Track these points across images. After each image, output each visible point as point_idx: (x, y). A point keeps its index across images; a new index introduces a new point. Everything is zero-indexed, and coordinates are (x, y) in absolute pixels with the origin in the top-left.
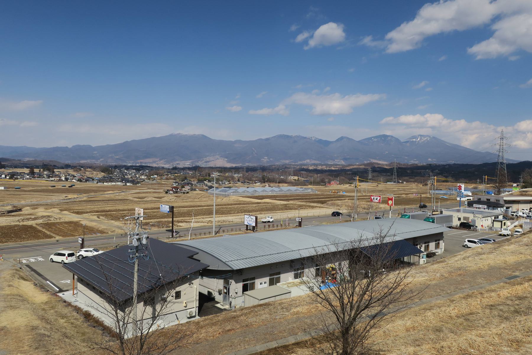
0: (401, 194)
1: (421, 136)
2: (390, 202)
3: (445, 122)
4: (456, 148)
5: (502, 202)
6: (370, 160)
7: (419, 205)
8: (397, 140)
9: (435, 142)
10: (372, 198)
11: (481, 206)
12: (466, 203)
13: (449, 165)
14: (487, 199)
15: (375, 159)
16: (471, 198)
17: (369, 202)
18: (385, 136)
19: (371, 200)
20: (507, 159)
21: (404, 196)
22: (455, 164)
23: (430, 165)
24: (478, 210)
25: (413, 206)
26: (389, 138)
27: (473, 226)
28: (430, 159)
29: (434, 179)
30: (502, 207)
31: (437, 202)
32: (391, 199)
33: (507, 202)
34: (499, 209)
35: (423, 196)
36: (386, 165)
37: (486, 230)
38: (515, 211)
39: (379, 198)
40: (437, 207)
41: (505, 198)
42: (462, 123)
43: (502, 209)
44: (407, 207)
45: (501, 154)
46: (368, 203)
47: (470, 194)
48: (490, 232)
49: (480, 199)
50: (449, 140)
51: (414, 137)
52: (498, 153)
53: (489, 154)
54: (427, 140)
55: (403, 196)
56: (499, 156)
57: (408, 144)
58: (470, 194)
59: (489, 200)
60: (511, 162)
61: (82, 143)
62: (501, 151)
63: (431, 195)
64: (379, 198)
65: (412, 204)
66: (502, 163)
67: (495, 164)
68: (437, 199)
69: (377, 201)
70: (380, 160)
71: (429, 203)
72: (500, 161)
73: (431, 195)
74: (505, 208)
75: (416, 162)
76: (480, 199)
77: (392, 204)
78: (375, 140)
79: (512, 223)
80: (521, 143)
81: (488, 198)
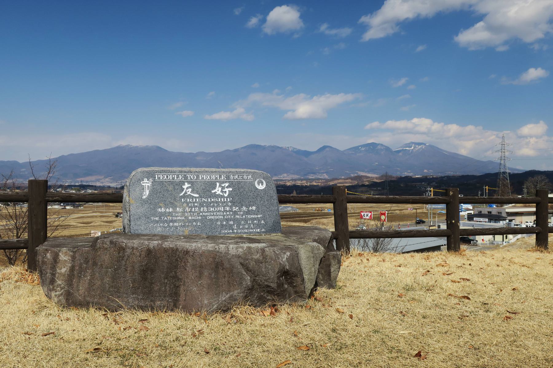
0: (395, 210)
1: (416, 144)
2: (383, 217)
3: (436, 127)
4: (455, 157)
5: (504, 215)
6: (357, 173)
7: (414, 221)
8: (387, 149)
9: (433, 150)
10: (362, 214)
11: (481, 219)
12: (466, 217)
13: (448, 177)
14: (488, 212)
15: (363, 171)
16: (472, 212)
17: (358, 219)
18: (374, 145)
19: (361, 217)
20: (509, 169)
21: (398, 212)
22: (453, 176)
23: (426, 177)
24: (478, 223)
25: (408, 223)
26: (379, 147)
27: (473, 240)
28: (425, 171)
29: (430, 191)
30: (504, 220)
31: (434, 217)
32: (384, 214)
33: (509, 214)
34: (501, 222)
35: (419, 211)
36: (376, 178)
37: (486, 244)
38: (518, 223)
39: (370, 214)
40: (434, 222)
41: (507, 210)
42: (454, 128)
43: (505, 222)
44: (401, 223)
45: (502, 162)
46: (359, 221)
47: (471, 208)
48: (491, 246)
49: (481, 212)
50: (445, 147)
51: (409, 145)
52: (499, 161)
53: (491, 162)
54: (421, 148)
55: (396, 212)
56: (501, 164)
57: (400, 154)
58: (471, 208)
59: (491, 212)
60: (516, 172)
61: (488, 172)
62: (503, 158)
63: (428, 210)
64: (370, 214)
65: (407, 220)
66: (504, 173)
67: (497, 175)
68: (434, 214)
69: (368, 218)
70: (369, 172)
71: (426, 218)
72: (502, 171)
73: (428, 210)
74: (507, 221)
75: (410, 174)
76: (481, 212)
77: (385, 220)
78: (363, 149)
79: (514, 237)
80: (527, 151)
81: (490, 210)
